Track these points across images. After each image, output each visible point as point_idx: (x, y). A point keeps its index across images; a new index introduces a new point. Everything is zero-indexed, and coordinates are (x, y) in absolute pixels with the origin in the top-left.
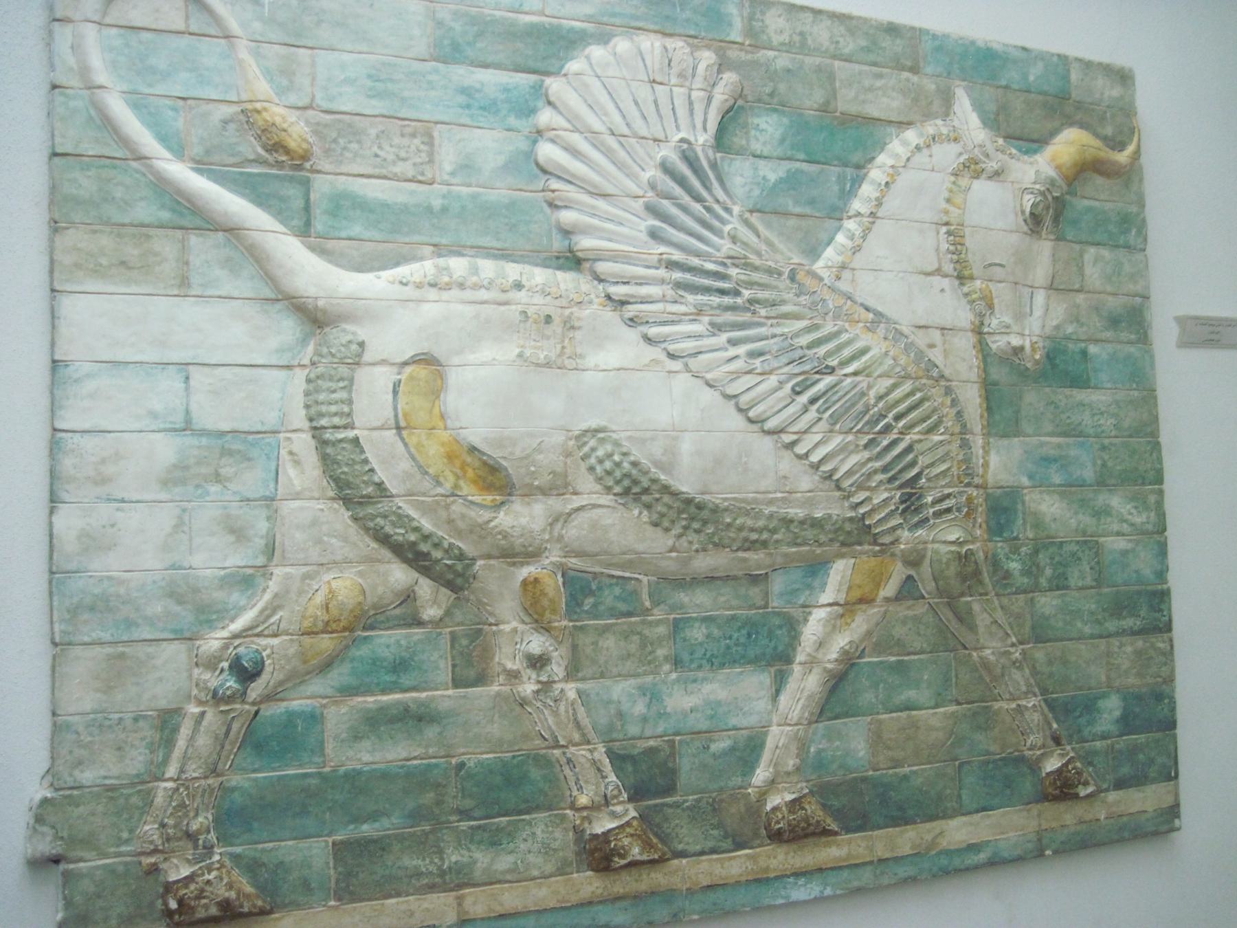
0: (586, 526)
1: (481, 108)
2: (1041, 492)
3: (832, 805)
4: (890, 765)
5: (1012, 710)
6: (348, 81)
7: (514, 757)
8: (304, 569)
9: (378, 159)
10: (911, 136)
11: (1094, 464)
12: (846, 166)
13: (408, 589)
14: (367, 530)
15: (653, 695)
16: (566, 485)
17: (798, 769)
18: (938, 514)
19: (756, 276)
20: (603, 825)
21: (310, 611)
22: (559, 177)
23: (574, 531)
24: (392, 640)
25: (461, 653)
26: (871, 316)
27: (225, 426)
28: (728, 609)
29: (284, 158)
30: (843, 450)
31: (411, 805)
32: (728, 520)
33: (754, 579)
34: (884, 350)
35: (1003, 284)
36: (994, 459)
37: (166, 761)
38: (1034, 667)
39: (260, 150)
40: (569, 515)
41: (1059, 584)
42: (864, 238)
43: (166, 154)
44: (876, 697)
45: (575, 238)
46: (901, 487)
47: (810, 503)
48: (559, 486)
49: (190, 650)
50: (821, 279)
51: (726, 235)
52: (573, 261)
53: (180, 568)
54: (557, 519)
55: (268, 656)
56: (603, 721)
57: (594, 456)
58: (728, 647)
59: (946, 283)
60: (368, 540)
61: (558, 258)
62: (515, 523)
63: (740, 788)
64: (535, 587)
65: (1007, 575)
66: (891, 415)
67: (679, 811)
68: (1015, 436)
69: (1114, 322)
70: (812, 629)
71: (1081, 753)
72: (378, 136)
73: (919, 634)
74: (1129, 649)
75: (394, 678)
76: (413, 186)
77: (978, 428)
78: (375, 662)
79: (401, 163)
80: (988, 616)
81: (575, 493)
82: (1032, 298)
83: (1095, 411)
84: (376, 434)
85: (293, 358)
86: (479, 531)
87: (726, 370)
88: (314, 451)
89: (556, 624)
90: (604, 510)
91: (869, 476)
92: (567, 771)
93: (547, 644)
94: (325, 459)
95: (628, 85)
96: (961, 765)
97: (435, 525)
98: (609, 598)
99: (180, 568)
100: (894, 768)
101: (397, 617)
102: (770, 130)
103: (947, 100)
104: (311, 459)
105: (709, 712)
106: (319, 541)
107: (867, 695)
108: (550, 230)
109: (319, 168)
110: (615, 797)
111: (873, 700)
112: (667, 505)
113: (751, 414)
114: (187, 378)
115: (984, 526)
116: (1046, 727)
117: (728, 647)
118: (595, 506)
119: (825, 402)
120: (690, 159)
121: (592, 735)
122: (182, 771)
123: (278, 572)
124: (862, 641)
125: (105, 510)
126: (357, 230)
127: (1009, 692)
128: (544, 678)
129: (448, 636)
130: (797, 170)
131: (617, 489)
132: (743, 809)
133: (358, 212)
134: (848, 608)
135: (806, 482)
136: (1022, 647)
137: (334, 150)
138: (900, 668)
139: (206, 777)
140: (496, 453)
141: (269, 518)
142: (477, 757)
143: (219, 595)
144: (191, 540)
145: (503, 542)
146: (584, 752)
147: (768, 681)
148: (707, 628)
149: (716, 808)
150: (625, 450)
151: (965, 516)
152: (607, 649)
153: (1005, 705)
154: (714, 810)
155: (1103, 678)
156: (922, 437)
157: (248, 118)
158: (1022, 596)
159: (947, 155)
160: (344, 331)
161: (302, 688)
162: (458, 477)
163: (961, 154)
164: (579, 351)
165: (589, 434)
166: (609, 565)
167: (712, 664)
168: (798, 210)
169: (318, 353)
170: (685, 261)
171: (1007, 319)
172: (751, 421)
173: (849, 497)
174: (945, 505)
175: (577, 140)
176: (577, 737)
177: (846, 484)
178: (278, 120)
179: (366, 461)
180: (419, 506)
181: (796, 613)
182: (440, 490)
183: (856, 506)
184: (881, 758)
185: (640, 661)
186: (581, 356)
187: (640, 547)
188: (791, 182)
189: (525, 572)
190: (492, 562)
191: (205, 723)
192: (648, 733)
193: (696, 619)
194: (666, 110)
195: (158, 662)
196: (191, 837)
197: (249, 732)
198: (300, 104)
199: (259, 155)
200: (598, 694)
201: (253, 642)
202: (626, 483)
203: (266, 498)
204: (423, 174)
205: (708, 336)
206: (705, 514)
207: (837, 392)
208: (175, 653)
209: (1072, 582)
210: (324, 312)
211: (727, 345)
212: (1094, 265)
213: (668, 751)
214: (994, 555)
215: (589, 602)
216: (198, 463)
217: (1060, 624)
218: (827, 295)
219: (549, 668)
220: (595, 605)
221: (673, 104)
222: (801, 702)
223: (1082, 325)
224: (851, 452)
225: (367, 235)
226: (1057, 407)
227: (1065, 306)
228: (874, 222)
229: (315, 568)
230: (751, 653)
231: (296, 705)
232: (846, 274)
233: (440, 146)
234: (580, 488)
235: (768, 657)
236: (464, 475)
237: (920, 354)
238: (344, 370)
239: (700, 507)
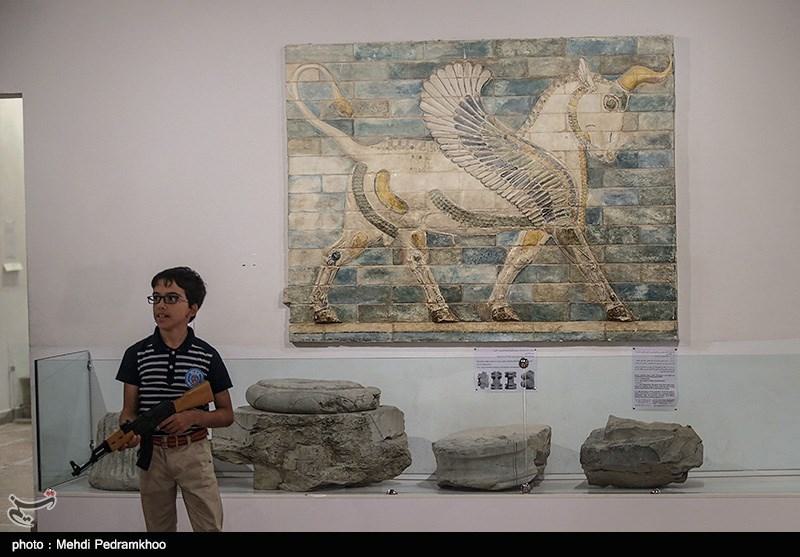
15: (455, 272)
18: (559, 216)
23: (427, 221)
30: (518, 194)
31: (380, 297)
36: (590, 196)
41: (618, 242)
48: (424, 207)
52: (431, 138)
59: (568, 134)
65: (594, 238)
69: (653, 141)
70: (511, 253)
74: (652, 268)
78: (371, 257)
91: (529, 204)
98: (441, 241)
103: (577, 63)
106: (354, 222)
125: (301, 215)
126: (367, 134)
134: (524, 247)
135: (505, 205)
138: (546, 268)
142: (398, 285)
158: (600, 247)
177: (520, 206)
181: (507, 248)
188: (509, 103)
196: (322, 301)
208: (319, 252)
215: (435, 242)
231: (350, 267)
237: (553, 161)
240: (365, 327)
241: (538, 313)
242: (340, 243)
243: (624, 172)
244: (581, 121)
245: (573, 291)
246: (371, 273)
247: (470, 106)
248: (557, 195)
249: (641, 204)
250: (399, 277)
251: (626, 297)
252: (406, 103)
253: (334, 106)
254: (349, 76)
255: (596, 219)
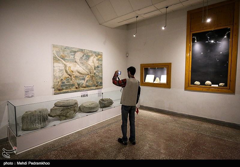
48: (75, 72)
134: (87, 78)
142: (71, 84)
159: (93, 57)
188: (86, 58)
208: (59, 79)
240: (66, 90)
242: (63, 78)
244: (94, 62)
247: (81, 58)
248: (92, 71)
250: (71, 82)
252: (72, 56)
253: (62, 55)
254: (64, 51)
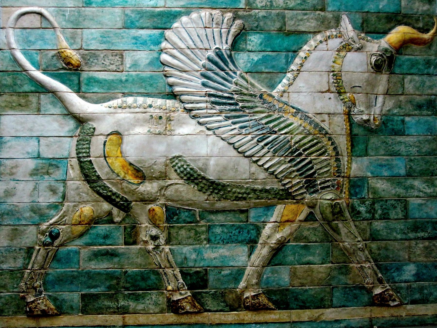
0: (173, 191)
1: (141, 44)
2: (377, 179)
3: (272, 299)
4: (299, 285)
5: (359, 267)
6: (94, 39)
7: (145, 270)
8: (74, 204)
9: (104, 65)
10: (319, 37)
11: (406, 167)
12: (289, 52)
13: (109, 211)
14: (95, 191)
15: (199, 252)
16: (166, 176)
17: (257, 284)
18: (322, 188)
19: (245, 98)
20: (176, 297)
21: (75, 217)
22: (168, 66)
23: (168, 193)
24: (104, 228)
25: (128, 234)
26: (295, 110)
27: (50, 156)
28: (231, 222)
29: (71, 67)
30: (279, 163)
31: (108, 284)
32: (229, 189)
33: (242, 212)
34: (299, 124)
35: (360, 94)
36: (354, 166)
37: (28, 264)
38: (371, 250)
39: (64, 65)
40: (167, 187)
41: (385, 217)
42: (294, 79)
43: (34, 69)
44: (294, 258)
45: (174, 88)
46: (305, 178)
47: (265, 183)
48: (163, 176)
49: (37, 228)
50: (274, 97)
51: (233, 82)
52: (174, 96)
53: (35, 202)
54: (162, 188)
55: (61, 232)
56: (179, 260)
57: (177, 166)
58: (230, 236)
59: (332, 95)
60: (95, 194)
61: (168, 95)
62: (145, 190)
63: (234, 288)
64: (153, 212)
65: (359, 212)
66: (301, 149)
67: (208, 295)
68: (365, 156)
70: (267, 230)
71: (394, 287)
72: (104, 57)
73: (315, 235)
75: (104, 241)
76: (116, 73)
77: (345, 154)
78: (98, 235)
79: (111, 66)
80: (346, 229)
81: (170, 179)
82: (376, 99)
83: (407, 145)
84: (98, 159)
85: (73, 134)
86: (133, 192)
87: (230, 134)
88: (78, 165)
89: (161, 225)
90: (180, 185)
91: (291, 173)
92: (165, 277)
93: (158, 232)
94: (82, 168)
95: (196, 30)
96: (333, 288)
97: (117, 190)
98: (184, 215)
99: (35, 202)
100: (302, 286)
101: (105, 220)
102: (256, 40)
104: (77, 167)
105: (222, 260)
106: (79, 194)
107: (290, 257)
108: (165, 85)
109: (83, 69)
110: (181, 288)
111: (293, 259)
112: (204, 184)
113: (239, 150)
114: (39, 141)
115: (347, 193)
116: (375, 276)
117: (230, 236)
118: (177, 184)
119: (271, 145)
120: (219, 54)
121: (174, 265)
122: (33, 267)
123: (66, 204)
124: (288, 237)
126: (96, 89)
127: (357, 260)
128: (156, 244)
129: (123, 228)
130: (267, 55)
131: (185, 178)
132: (234, 296)
133: (96, 83)
134: (281, 223)
135: (262, 175)
136: (364, 242)
137: (88, 63)
139: (40, 270)
140: (139, 166)
141: (64, 187)
143: (47, 211)
144: (39, 193)
145: (141, 196)
146: (170, 271)
147: (247, 249)
148: (222, 229)
149: (223, 295)
150: (188, 164)
151: (336, 189)
152: (182, 234)
153: (355, 265)
154: (222, 296)
155: (407, 257)
156: (316, 158)
157: (60, 55)
158: (366, 222)
159: (335, 43)
160: (89, 124)
161: (73, 243)
162: (126, 174)
163: (342, 42)
164: (172, 128)
165: (175, 158)
166: (183, 205)
167: (223, 242)
168: (267, 70)
169: (80, 132)
170: (216, 94)
171: (362, 109)
172: (239, 152)
173: (281, 182)
174: (326, 185)
175: (175, 52)
176: (168, 265)
177: (280, 176)
178: (69, 54)
179: (94, 168)
180: (112, 183)
182: (119, 178)
183: (284, 185)
184: (295, 282)
185: (194, 239)
186: (173, 130)
187: (194, 199)
188: (264, 61)
189: (150, 206)
190: (138, 203)
191: (40, 252)
192: (197, 266)
193: (218, 225)
194: (210, 38)
195: (28, 232)
196: (35, 288)
197: (55, 256)
198: (77, 48)
199: (63, 66)
200: (177, 251)
201: (57, 227)
202: (188, 175)
203: (63, 180)
204: (119, 69)
205: (224, 121)
206: (220, 187)
207: (277, 141)
208: (32, 229)
209: (391, 216)
210: (82, 118)
211: (231, 124)
212: (410, 84)
213: (204, 273)
214: (352, 205)
215: (175, 218)
216: (42, 169)
217: (385, 234)
218: (276, 103)
219: (158, 240)
220: (178, 219)
221: (214, 35)
222: (260, 258)
223: (402, 109)
224: (283, 164)
225: (99, 91)
226: (387, 144)
227: (393, 101)
228: (299, 73)
229: (77, 203)
230: (240, 239)
231: (69, 248)
232: (286, 95)
233: (125, 58)
234: (171, 177)
235: (247, 240)
236: (128, 173)
237: (317, 125)
238: (88, 137)
239: (218, 184)
241: (296, 299)
243: (390, 139)
245: (335, 273)
246: (96, 255)
249: (409, 175)
251: (393, 278)
255: (361, 191)
